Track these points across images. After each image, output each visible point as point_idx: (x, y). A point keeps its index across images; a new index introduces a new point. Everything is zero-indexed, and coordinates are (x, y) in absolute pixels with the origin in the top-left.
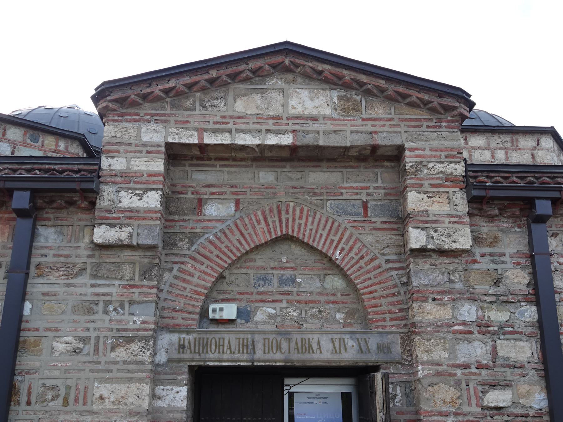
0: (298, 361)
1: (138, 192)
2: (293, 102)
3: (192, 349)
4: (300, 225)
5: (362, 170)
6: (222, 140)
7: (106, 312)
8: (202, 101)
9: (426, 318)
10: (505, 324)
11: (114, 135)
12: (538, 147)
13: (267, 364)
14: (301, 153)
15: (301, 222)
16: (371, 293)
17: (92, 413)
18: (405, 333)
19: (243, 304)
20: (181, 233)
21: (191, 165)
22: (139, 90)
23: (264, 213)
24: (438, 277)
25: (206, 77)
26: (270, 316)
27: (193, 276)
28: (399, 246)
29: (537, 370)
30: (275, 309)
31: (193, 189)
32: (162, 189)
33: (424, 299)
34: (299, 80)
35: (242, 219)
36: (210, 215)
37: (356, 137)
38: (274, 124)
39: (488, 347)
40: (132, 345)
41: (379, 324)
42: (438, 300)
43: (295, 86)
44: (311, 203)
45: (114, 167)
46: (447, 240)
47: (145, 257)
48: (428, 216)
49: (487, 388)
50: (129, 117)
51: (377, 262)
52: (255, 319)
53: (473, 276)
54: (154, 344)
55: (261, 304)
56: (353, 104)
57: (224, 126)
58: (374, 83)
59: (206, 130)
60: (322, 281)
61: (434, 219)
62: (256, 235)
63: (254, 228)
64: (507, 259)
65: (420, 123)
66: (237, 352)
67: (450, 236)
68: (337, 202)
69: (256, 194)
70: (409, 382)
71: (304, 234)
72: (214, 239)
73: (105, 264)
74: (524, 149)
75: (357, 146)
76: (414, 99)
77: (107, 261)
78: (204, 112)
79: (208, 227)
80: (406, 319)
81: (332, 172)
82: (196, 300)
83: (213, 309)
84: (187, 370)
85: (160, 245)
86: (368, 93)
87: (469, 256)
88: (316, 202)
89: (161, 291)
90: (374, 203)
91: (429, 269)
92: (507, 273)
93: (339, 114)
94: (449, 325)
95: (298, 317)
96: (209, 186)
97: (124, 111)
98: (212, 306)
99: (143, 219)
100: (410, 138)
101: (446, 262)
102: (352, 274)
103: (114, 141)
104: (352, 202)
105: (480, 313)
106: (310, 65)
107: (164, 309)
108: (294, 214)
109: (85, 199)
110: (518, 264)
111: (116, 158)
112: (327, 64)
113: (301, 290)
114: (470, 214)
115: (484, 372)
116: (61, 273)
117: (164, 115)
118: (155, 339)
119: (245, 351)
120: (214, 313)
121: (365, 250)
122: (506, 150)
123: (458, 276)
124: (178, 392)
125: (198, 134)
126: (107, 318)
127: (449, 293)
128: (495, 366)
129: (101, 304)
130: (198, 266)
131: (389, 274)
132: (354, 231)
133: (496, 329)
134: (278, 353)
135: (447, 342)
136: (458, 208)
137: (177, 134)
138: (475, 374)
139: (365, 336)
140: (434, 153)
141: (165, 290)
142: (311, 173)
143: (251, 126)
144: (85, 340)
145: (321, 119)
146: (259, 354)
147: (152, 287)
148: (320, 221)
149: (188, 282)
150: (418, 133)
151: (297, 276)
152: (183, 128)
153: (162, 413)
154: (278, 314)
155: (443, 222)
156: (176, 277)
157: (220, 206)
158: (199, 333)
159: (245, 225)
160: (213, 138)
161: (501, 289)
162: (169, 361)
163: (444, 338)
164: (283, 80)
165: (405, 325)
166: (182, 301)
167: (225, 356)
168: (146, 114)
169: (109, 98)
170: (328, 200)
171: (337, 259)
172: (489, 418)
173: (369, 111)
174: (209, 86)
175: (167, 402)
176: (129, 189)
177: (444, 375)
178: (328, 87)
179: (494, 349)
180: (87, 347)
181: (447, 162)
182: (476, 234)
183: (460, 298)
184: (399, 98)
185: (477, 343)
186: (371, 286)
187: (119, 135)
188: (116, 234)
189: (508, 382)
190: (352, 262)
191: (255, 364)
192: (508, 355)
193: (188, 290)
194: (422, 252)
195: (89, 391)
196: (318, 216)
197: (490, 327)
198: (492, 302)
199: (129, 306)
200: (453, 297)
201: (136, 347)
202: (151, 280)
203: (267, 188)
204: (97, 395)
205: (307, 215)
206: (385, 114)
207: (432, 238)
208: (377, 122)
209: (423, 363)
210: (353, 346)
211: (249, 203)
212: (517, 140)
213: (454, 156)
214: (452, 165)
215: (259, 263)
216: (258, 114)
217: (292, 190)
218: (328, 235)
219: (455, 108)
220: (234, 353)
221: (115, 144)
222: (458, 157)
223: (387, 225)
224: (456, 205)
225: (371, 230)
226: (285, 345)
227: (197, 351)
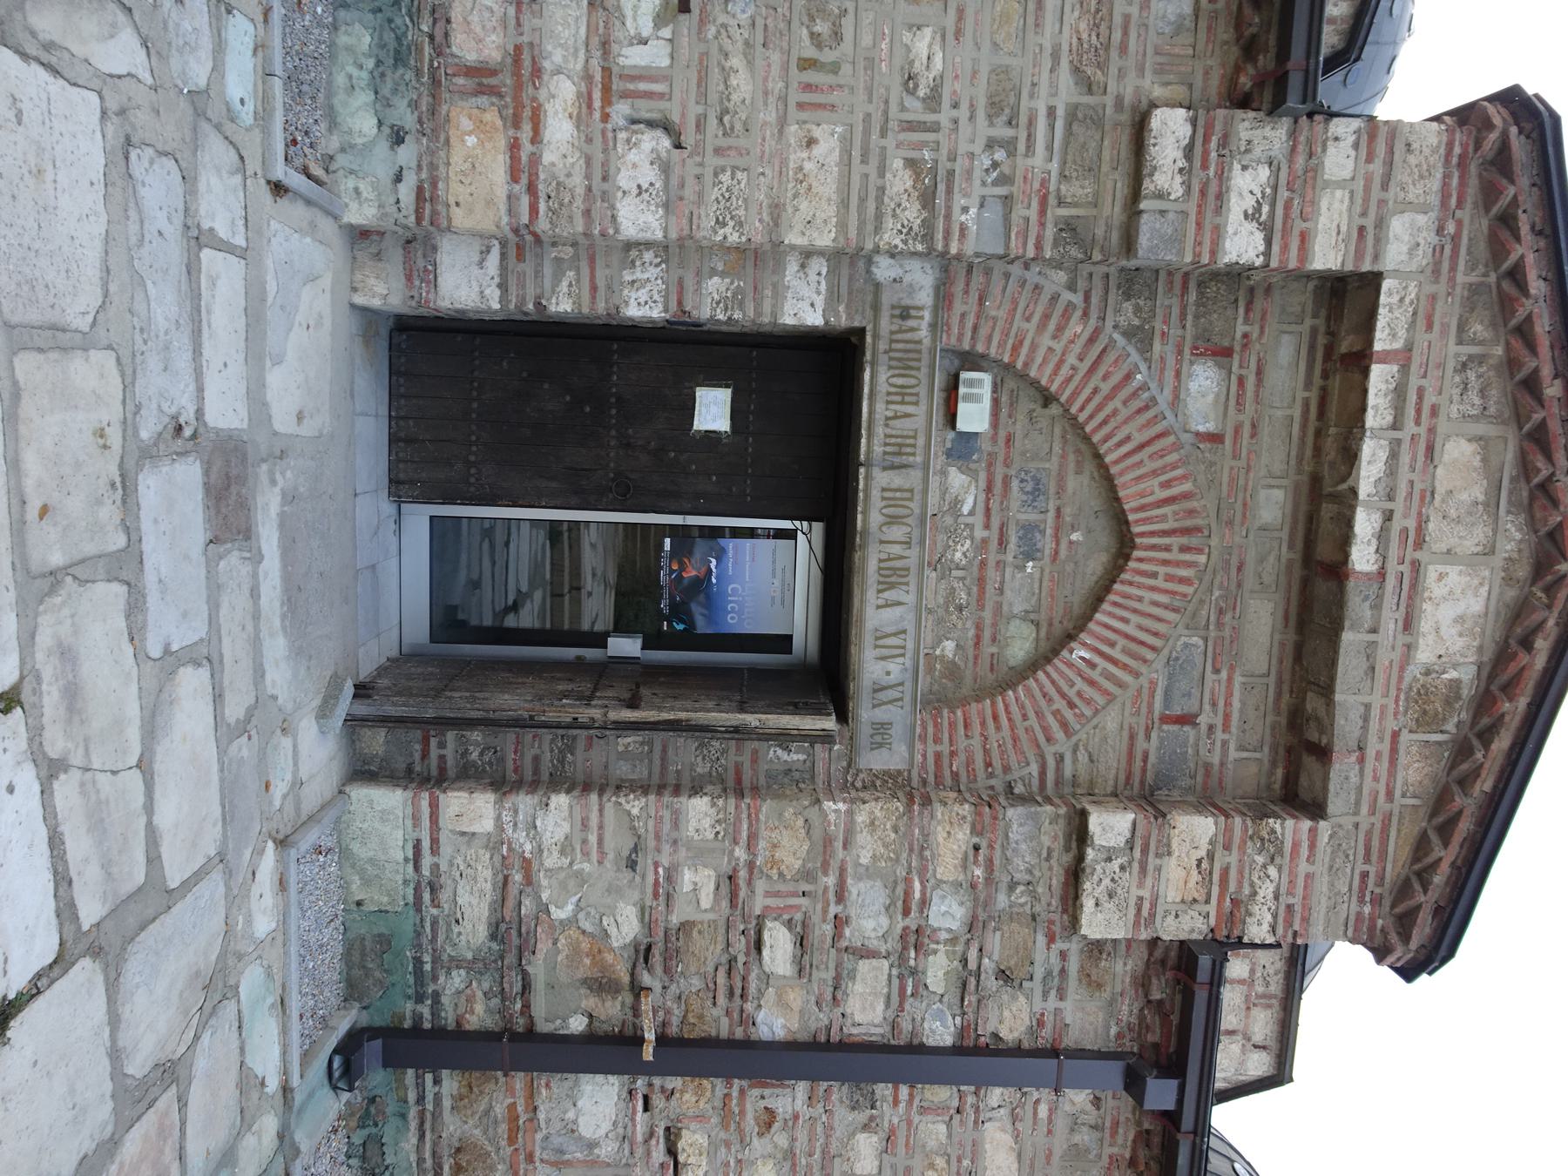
0: (864, 559)
1: (1265, 209)
2: (1455, 576)
3: (899, 336)
4: (1154, 575)
5: (1270, 719)
6: (1376, 407)
7: (991, 145)
8: (1481, 359)
11: (1414, 146)
12: (1249, 1046)
13: (861, 495)
14: (1322, 587)
15: (1161, 577)
16: (995, 717)
17: (782, 123)
18: (909, 780)
19: (986, 446)
20: (1153, 310)
21: (1314, 332)
22: (1528, 206)
23: (1186, 496)
24: (1022, 861)
25: (1546, 371)
26: (957, 503)
27: (1055, 337)
28: (1092, 783)
29: (829, 1029)
30: (971, 513)
31: (1255, 336)
32: (1266, 265)
33: (979, 827)
34: (1512, 594)
35: (1177, 447)
36: (1190, 376)
37: (1355, 716)
38: (1405, 530)
39: (875, 942)
40: (917, 206)
41: (930, 730)
43: (1498, 581)
44: (1202, 602)
45: (1332, 149)
47: (1109, 227)
48: (1157, 855)
49: (799, 929)
50: (1455, 182)
51: (1059, 734)
52: (953, 471)
53: (1021, 932)
54: (915, 254)
55: (982, 484)
56: (1436, 714)
57: (1410, 412)
58: (1486, 766)
59: (1405, 369)
60: (1025, 617)
61: (1150, 867)
62: (1139, 479)
63: (1155, 473)
64: (1052, 1002)
65: (1374, 857)
66: (888, 431)
67: (1110, 896)
68: (1199, 660)
69: (1231, 479)
70: (813, 777)
71: (1131, 584)
72: (1135, 384)
73: (1098, 137)
74: (1247, 1017)
75: (1331, 714)
76: (1438, 851)
77: (1106, 143)
78: (1451, 365)
79: (1162, 370)
80: (937, 784)
82: (1002, 345)
83: (980, 381)
84: (856, 324)
85: (1133, 263)
86: (1462, 750)
87: (1064, 928)
88: (1204, 613)
89: (1027, 266)
90: (1191, 740)
91: (1040, 844)
92: (1022, 999)
93: (1415, 679)
94: (922, 872)
95: (952, 561)
96: (1259, 372)
97: (1473, 169)
98: (986, 378)
100: (1341, 833)
101: (1054, 882)
102: (1036, 680)
103: (1399, 148)
104: (1196, 692)
105: (944, 936)
106: (1551, 623)
107: (988, 272)
108: (1178, 564)
109: (1259, 84)
110: (1041, 1023)
111: (1353, 153)
112: (1548, 662)
113: (1008, 571)
114: (1154, 942)
115: (828, 928)
116: (1085, 36)
117: (1453, 269)
118: (926, 255)
119: (888, 449)
120: (971, 383)
121: (1088, 712)
122: (1249, 982)
123: (1022, 900)
124: (812, 305)
125: (1396, 352)
126: (978, 148)
127: (989, 880)
129: (1009, 132)
130: (1077, 348)
131: (1032, 758)
132: (1131, 692)
133: (912, 963)
134: (881, 519)
136: (1170, 919)
137: (1402, 300)
138: (825, 911)
139: (907, 698)
140: (1300, 882)
141: (1028, 275)
142: (1271, 605)
143: (1404, 475)
144: (933, 100)
145: (1408, 639)
146: (881, 478)
147: (1039, 246)
148: (1160, 620)
149: (1042, 326)
150: (1351, 852)
151: (1039, 564)
152: (1415, 314)
153: (774, 272)
154: (961, 520)
155: (1141, 885)
156: (1055, 298)
157: (1211, 398)
158: (932, 351)
159: (1161, 454)
160: (1384, 387)
161: (990, 983)
162: (877, 286)
163: (897, 860)
164: (1515, 555)
165: (924, 782)
166: (1002, 314)
167: (880, 407)
168: (1459, 223)
169: (1514, 130)
170: (1206, 640)
171: (1071, 652)
172: (742, 927)
173: (1414, 749)
174: (1519, 376)
175: (794, 283)
176: (1275, 188)
178: (1485, 659)
180: (918, 105)
182: (1109, 947)
183: (976, 900)
184: (1440, 819)
185: (884, 921)
186: (1010, 720)
187: (1412, 160)
188: (1169, 160)
190: (1062, 683)
191: (862, 470)
192: (858, 977)
193: (1026, 325)
194: (1079, 834)
195: (826, 114)
198: (964, 961)
199: (1000, 197)
200: (980, 887)
201: (912, 213)
203: (1245, 505)
204: (817, 132)
205: (1174, 593)
206: (1406, 783)
207: (1109, 859)
208: (1385, 764)
209: (850, 813)
210: (888, 673)
211: (1212, 464)
212: (1269, 1006)
213: (1289, 923)
214: (1269, 917)
215: (1072, 483)
216: (1433, 493)
217: (1234, 561)
218: (1127, 636)
219: (1405, 938)
220: (887, 425)
221: (1391, 151)
222: (1286, 931)
223: (1138, 763)
224: (1177, 916)
226: (897, 532)
227: (894, 346)
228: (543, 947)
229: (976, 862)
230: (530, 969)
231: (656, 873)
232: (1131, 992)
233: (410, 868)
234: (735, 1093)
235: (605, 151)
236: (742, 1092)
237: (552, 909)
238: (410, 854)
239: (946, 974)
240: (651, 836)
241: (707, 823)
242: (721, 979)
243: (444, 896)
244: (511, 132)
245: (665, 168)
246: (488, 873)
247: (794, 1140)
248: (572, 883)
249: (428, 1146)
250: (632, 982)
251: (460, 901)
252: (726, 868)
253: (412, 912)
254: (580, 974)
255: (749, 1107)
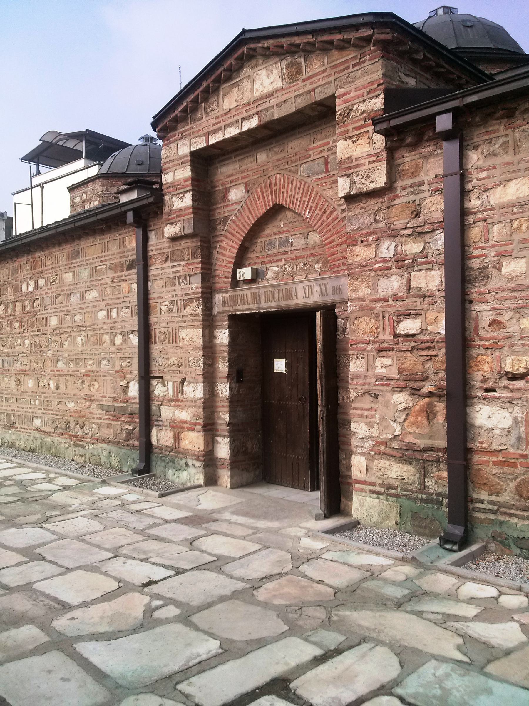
4: (283, 192)
9: (356, 260)
10: (418, 256)
23: (261, 190)
24: (367, 219)
26: (277, 273)
30: (277, 266)
31: (221, 182)
33: (354, 243)
37: (299, 100)
41: (335, 269)
42: (365, 241)
46: (366, 182)
49: (401, 317)
51: (335, 214)
52: (268, 277)
56: (296, 68)
59: (209, 133)
61: (357, 163)
68: (307, 164)
71: (286, 201)
79: (231, 210)
81: (303, 137)
92: (425, 203)
94: (372, 264)
99: (185, 215)
101: (372, 203)
106: (260, 45)
116: (159, 261)
126: (180, 287)
128: (407, 297)
134: (273, 301)
135: (370, 280)
136: (376, 146)
138: (390, 306)
144: (172, 302)
146: (263, 304)
149: (223, 255)
155: (364, 165)
157: (236, 191)
161: (421, 219)
167: (246, 307)
170: (301, 165)
172: (401, 344)
177: (367, 310)
179: (409, 280)
181: (369, 98)
185: (394, 277)
186: (331, 237)
189: (418, 311)
192: (420, 286)
196: (295, 181)
197: (404, 261)
198: (409, 236)
201: (195, 304)
202: (197, 258)
203: (262, 167)
204: (181, 337)
206: (320, 67)
208: (314, 79)
214: (373, 101)
218: (302, 197)
222: (378, 90)
225: (331, 184)
228: (411, 439)
229: (367, 241)
230: (422, 446)
231: (378, 385)
232: (419, 150)
233: (381, 497)
234: (482, 343)
235: (187, 401)
236: (481, 339)
237: (397, 433)
238: (375, 496)
239: (414, 243)
240: (364, 387)
241: (358, 363)
242: (425, 353)
243: (395, 483)
244: (185, 430)
245: (190, 383)
246: (383, 461)
247: (508, 309)
248: (385, 424)
249: (519, 512)
250: (429, 397)
251: (395, 477)
252: (375, 353)
253: (400, 500)
254: (425, 422)
255: (488, 335)
